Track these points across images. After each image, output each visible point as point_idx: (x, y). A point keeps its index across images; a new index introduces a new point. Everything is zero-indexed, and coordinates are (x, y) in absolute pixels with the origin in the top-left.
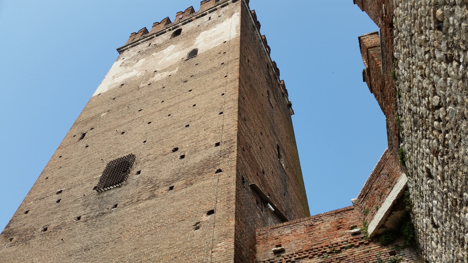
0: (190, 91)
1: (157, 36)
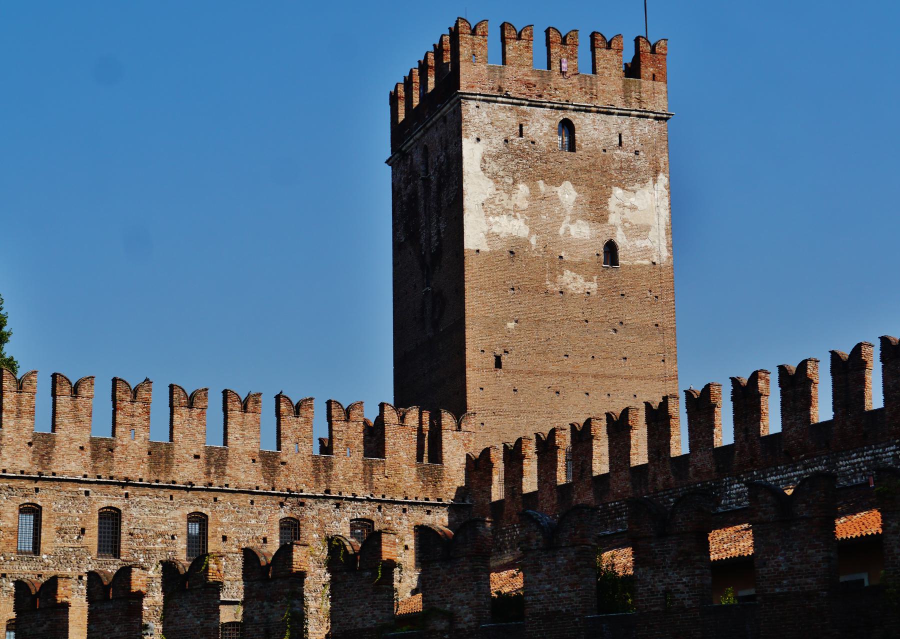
0: (625, 358)
1: (529, 105)
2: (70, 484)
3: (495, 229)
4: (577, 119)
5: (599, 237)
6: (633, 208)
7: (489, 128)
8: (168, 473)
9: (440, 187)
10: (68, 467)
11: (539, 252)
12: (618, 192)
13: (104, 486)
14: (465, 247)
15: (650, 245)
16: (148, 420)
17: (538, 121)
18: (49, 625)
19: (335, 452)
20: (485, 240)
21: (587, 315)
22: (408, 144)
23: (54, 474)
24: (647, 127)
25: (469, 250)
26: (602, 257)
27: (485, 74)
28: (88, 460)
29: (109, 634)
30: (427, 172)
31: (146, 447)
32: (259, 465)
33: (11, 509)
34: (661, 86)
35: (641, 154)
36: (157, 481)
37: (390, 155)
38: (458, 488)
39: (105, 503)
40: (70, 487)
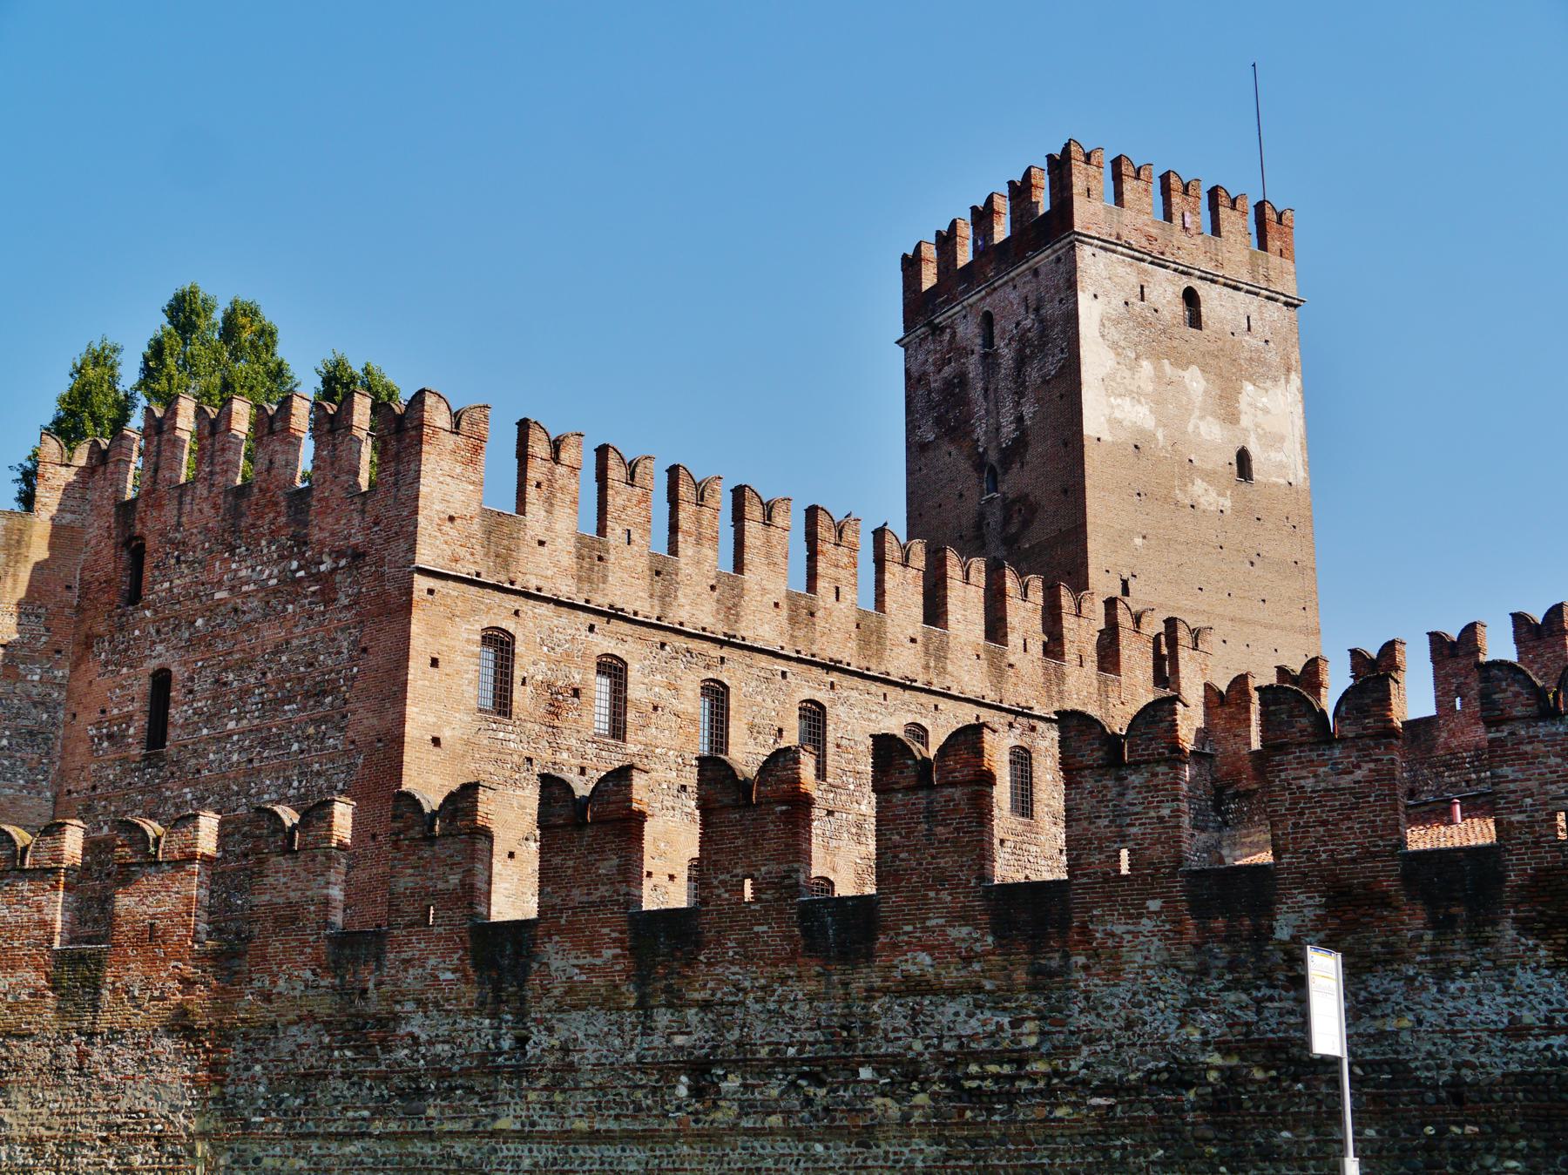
1: (1151, 263)
2: (764, 657)
3: (1118, 414)
4: (1203, 289)
5: (1231, 441)
6: (1266, 411)
7: (1107, 284)
8: (880, 657)
9: (1021, 362)
10: (760, 631)
11: (1167, 451)
13: (804, 666)
14: (1086, 431)
15: (1285, 459)
16: (854, 575)
17: (1160, 285)
18: (1371, 770)
19: (1067, 658)
20: (1106, 426)
21: (1221, 540)
22: (949, 313)
23: (744, 639)
24: (1275, 311)
25: (1089, 437)
26: (1235, 467)
27: (1102, 216)
28: (785, 624)
29: (1561, 784)
30: (988, 340)
31: (854, 617)
32: (984, 663)
33: (691, 684)
34: (1288, 264)
35: (1271, 344)
36: (868, 669)
37: (901, 334)
38: (1199, 730)
39: (807, 694)
40: (763, 661)
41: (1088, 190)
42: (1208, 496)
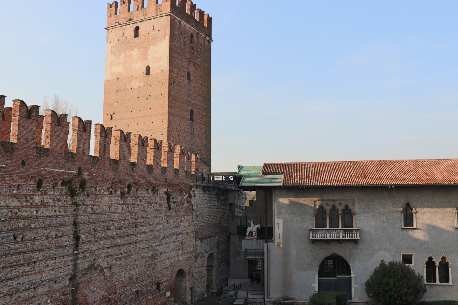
1: (126, 25)
12: (152, 47)
41: (111, 14)
42: (135, 84)
